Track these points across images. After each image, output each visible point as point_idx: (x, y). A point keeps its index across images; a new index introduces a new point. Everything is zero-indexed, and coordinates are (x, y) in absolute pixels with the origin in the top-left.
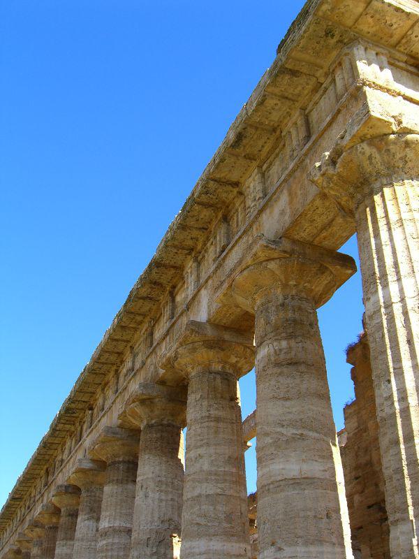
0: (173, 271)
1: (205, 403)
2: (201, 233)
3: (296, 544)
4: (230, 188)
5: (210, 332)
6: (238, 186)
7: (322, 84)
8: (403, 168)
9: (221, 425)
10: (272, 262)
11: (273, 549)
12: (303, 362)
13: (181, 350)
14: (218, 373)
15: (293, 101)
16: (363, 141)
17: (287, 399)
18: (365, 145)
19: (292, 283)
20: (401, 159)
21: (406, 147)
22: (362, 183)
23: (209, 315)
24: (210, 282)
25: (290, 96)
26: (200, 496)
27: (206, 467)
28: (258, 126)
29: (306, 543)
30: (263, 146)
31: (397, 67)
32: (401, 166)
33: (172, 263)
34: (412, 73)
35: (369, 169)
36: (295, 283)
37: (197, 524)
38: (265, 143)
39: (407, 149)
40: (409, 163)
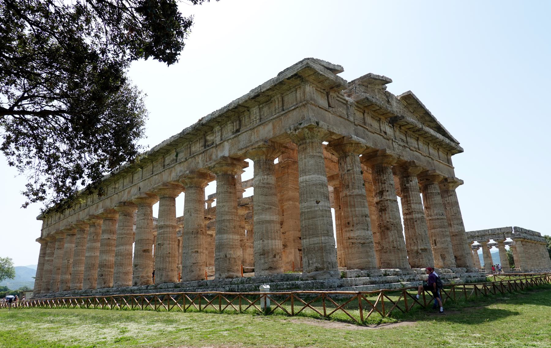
1: (226, 186)
5: (229, 161)
9: (232, 195)
13: (216, 165)
14: (230, 175)
23: (229, 154)
24: (230, 141)
27: (227, 210)
29: (272, 239)
35: (306, 136)
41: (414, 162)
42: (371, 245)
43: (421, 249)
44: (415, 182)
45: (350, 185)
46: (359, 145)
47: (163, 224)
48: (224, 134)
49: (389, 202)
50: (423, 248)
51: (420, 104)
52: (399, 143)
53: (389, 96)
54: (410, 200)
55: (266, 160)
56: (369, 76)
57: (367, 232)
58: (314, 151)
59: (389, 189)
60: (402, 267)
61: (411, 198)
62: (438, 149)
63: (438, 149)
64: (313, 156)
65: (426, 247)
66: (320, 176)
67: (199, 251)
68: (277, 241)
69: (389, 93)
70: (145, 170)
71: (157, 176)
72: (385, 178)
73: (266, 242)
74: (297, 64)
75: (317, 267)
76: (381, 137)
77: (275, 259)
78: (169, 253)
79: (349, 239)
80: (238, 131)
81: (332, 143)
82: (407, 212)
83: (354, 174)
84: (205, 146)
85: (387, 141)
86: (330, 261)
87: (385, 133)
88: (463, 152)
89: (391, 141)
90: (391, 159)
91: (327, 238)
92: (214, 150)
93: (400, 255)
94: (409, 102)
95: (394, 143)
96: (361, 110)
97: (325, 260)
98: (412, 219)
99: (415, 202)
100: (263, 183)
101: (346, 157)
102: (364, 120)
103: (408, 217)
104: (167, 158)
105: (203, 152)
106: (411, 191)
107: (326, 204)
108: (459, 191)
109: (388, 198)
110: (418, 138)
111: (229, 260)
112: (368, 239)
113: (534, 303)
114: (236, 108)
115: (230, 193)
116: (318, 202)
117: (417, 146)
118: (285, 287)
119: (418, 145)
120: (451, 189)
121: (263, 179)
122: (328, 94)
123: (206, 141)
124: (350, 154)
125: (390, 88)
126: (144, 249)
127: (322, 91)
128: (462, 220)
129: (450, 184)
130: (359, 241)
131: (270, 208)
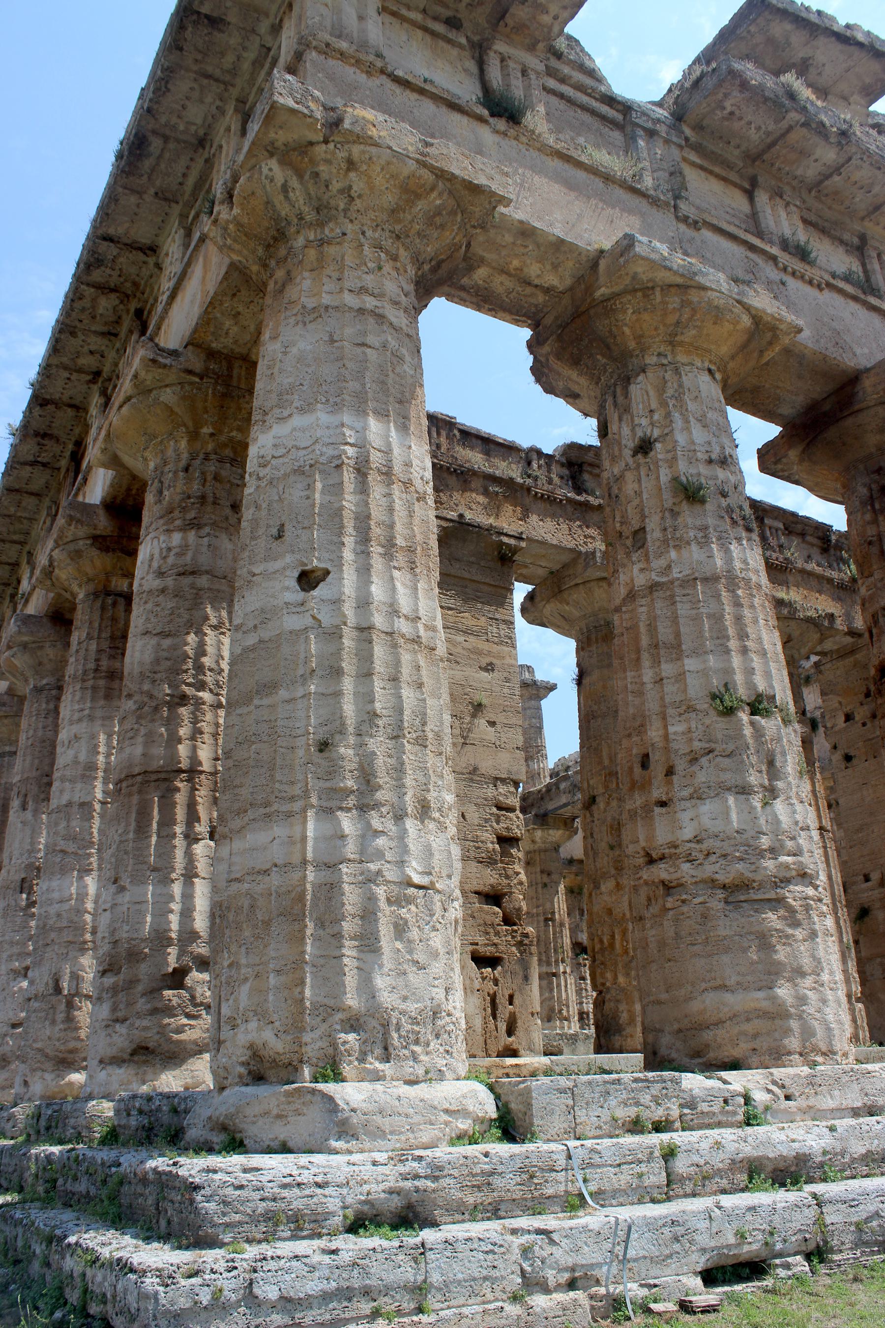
0: (70, 412)
2: (106, 342)
4: (141, 257)
6: (155, 251)
7: (269, 49)
8: (345, 211)
10: (168, 390)
12: (207, 572)
13: (56, 553)
15: (224, 83)
16: (272, 155)
18: (273, 163)
19: (206, 430)
20: (341, 191)
21: (348, 170)
22: (275, 239)
25: (217, 73)
26: (69, 804)
28: (168, 132)
30: (184, 175)
31: (403, 19)
32: (342, 206)
33: (65, 398)
35: (284, 210)
36: (211, 430)
37: (62, 851)
38: (188, 168)
39: (352, 175)
40: (358, 201)
46: (694, 296)
64: (318, 313)
81: (548, 321)
86: (352, 1000)
96: (733, 176)
101: (627, 380)
111: (70, 1005)
124: (650, 360)
130: (709, 869)
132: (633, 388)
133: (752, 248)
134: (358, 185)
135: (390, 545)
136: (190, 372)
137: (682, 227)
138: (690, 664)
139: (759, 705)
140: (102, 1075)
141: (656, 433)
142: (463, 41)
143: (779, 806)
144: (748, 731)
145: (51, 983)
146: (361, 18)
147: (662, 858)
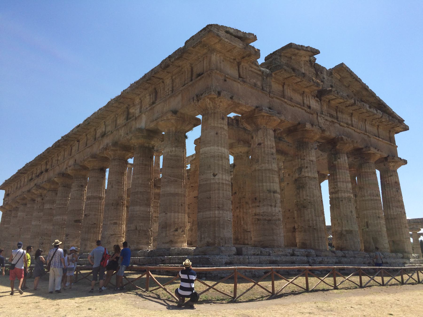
0: (129, 100)
3: (171, 212)
11: (164, 213)
17: (172, 168)
18: (208, 100)
24: (147, 113)
27: (140, 182)
29: (175, 212)
34: (231, 62)
35: (209, 106)
41: (342, 138)
42: (277, 222)
43: (346, 231)
44: (344, 161)
45: (260, 159)
47: (90, 195)
48: (143, 106)
49: (307, 178)
50: (347, 229)
51: (354, 78)
52: (326, 118)
53: (319, 69)
54: (337, 179)
55: (176, 132)
56: (290, 46)
57: (273, 209)
58: (216, 122)
59: (309, 165)
60: (317, 247)
61: (338, 177)
62: (378, 126)
63: (378, 126)
65: (351, 229)
66: (220, 148)
67: (118, 222)
68: (180, 214)
69: (319, 66)
70: (81, 143)
71: (89, 149)
72: (305, 154)
73: (169, 214)
74: (201, 31)
75: (208, 242)
76: (303, 111)
77: (176, 233)
78: (95, 224)
79: (255, 215)
80: (153, 103)
81: (244, 115)
82: (333, 190)
83: (264, 148)
84: (128, 118)
85: (311, 116)
86: (222, 236)
87: (309, 107)
88: (408, 129)
89: (315, 116)
90: (312, 134)
91: (221, 212)
92: (134, 123)
93: (316, 235)
94: (343, 75)
95: (319, 118)
97: (216, 235)
98: (338, 198)
99: (341, 180)
100: (171, 156)
101: (258, 130)
102: (284, 92)
103: (334, 195)
104: (98, 131)
105: (125, 125)
106: (339, 169)
107: (224, 177)
108: (401, 171)
109: (307, 175)
110: (352, 114)
112: (275, 215)
113: (43, 296)
114: (150, 79)
115: (146, 165)
116: (214, 175)
117: (350, 122)
118: (177, 261)
119: (352, 121)
120: (391, 168)
121: (171, 152)
122: (239, 64)
123: (128, 114)
124: (262, 127)
125: (320, 60)
126: (76, 219)
127: (232, 61)
128: (403, 202)
129: (391, 162)
130: (265, 217)
131: (176, 181)
132: (259, 132)
133: (282, 101)
134: (221, 104)
135: (225, 170)
136: (178, 117)
137: (270, 98)
138: (264, 184)
139: (275, 192)
140: (163, 245)
141: (262, 142)
142: (236, 63)
143: (277, 209)
144: (272, 196)
145: (135, 228)
146: (220, 63)
147: (258, 215)
